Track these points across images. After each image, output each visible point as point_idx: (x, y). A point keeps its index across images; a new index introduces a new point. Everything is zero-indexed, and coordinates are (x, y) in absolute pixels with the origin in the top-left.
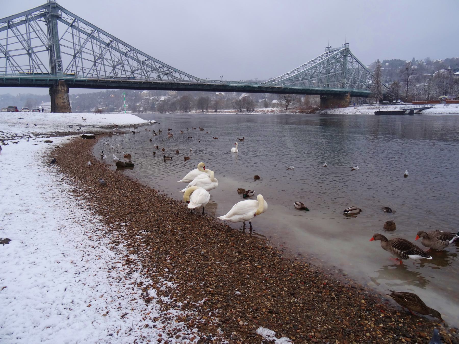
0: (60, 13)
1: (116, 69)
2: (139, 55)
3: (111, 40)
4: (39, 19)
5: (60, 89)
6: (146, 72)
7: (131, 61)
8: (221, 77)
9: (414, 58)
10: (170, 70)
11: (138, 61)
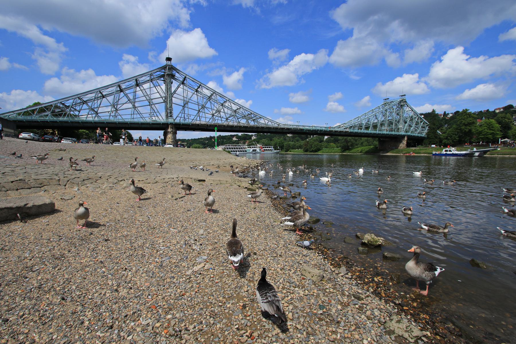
0: (174, 73)
2: (233, 105)
3: (212, 93)
6: (238, 119)
7: (226, 110)
10: (255, 117)
11: (231, 109)
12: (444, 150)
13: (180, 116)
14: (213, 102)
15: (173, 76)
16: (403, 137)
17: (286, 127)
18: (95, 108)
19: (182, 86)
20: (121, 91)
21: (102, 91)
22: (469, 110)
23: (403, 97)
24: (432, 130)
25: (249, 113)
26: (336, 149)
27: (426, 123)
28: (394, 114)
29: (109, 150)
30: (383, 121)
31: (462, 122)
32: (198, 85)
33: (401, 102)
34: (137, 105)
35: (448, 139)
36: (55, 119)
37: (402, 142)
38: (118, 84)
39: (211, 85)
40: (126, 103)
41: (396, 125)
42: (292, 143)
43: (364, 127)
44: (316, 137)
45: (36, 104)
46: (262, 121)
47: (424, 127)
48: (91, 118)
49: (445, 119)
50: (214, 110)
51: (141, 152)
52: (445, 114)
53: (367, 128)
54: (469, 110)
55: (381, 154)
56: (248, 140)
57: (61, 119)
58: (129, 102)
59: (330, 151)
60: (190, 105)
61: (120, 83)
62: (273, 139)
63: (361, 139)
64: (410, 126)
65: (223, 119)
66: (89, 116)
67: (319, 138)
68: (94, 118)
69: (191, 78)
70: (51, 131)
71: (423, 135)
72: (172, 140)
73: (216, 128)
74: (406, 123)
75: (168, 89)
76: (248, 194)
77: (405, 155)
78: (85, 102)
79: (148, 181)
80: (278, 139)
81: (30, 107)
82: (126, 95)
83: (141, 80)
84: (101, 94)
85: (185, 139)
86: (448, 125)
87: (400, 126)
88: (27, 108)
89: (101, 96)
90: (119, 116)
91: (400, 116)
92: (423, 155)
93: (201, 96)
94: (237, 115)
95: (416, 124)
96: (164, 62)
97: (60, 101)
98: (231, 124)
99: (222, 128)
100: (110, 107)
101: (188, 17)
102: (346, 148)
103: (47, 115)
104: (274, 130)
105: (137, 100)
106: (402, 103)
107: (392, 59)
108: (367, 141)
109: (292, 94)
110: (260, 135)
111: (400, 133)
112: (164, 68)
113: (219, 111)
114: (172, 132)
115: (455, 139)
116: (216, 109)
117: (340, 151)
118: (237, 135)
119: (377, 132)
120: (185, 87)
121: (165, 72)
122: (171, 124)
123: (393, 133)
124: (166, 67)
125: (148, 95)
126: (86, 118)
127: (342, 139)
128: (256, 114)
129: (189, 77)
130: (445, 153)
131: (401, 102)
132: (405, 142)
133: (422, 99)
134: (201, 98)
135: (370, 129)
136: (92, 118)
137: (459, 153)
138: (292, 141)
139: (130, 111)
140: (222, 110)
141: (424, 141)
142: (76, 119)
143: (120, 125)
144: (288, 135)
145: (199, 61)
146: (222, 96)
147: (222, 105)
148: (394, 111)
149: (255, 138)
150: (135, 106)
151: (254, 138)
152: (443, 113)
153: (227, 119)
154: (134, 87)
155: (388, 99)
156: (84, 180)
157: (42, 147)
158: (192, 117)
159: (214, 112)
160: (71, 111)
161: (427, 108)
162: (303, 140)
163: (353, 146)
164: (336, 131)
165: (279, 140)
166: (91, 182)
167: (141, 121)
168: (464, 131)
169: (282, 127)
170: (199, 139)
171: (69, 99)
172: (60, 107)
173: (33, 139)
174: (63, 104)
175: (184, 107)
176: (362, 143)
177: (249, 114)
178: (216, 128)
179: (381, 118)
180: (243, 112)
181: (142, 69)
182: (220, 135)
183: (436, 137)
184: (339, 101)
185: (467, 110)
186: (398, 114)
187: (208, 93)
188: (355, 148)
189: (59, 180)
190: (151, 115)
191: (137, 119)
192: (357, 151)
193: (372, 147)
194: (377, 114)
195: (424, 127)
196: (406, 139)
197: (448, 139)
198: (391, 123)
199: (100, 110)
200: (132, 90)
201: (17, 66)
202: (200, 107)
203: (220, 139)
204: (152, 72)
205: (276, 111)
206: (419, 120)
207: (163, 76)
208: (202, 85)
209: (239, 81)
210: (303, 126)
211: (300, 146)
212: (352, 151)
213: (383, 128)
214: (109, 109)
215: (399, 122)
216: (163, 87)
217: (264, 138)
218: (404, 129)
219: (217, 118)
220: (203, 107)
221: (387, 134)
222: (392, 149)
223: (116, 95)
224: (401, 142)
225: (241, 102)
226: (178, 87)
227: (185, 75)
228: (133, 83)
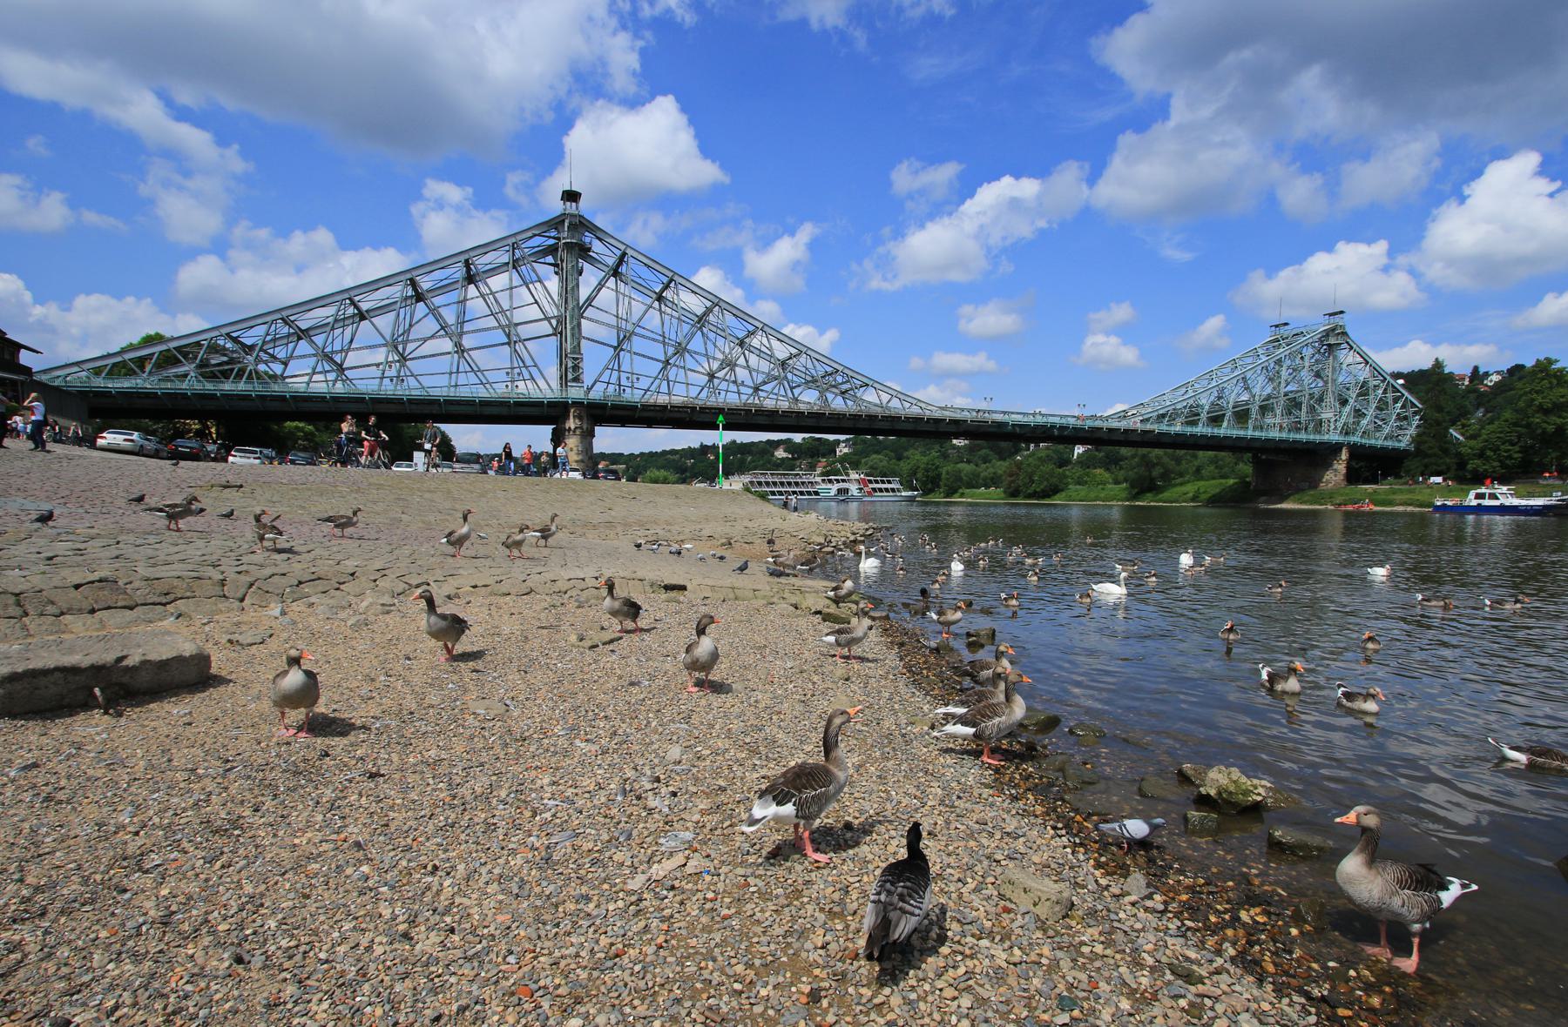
0: (587, 240)
1: (715, 380)
2: (775, 343)
3: (709, 304)
4: (542, 260)
5: (573, 427)
7: (753, 360)
8: (988, 399)
9: (1437, 359)
10: (849, 383)
11: (771, 357)
12: (1472, 494)
13: (605, 378)
14: (711, 335)
15: (583, 251)
16: (1335, 449)
17: (948, 415)
18: (337, 352)
19: (611, 282)
20: (419, 297)
21: (357, 299)
22: (1557, 361)
23: (1338, 320)
24: (1433, 429)
25: (829, 370)
26: (1111, 490)
27: (1413, 405)
28: (1307, 376)
29: (379, 487)
30: (1269, 397)
31: (1533, 400)
32: (665, 280)
33: (1327, 335)
34: (467, 342)
35: (1487, 459)
36: (209, 386)
37: (1331, 465)
38: (409, 276)
39: (707, 278)
40: (433, 337)
41: (1312, 409)
42: (966, 468)
43: (1204, 416)
44: (1047, 448)
45: (150, 340)
46: (870, 396)
47: (1406, 418)
48: (324, 386)
49: (1476, 391)
50: (714, 358)
51: (482, 495)
52: (1477, 376)
53: (1216, 420)
54: (1557, 361)
55: (1263, 506)
56: (824, 456)
57: (228, 386)
58: (442, 332)
59: (1092, 495)
60: (637, 344)
61: (415, 273)
62: (905, 454)
63: (1195, 457)
64: (1359, 414)
65: (743, 389)
66: (316, 378)
67: (1054, 451)
68: (331, 384)
69: (640, 257)
70: (195, 425)
71: (1402, 445)
72: (580, 457)
73: (721, 418)
74: (1344, 402)
75: (569, 291)
76: (826, 631)
77: (1343, 508)
78: (303, 334)
79: (504, 588)
80: (923, 454)
81: (131, 348)
82: (434, 312)
83: (482, 262)
84: (356, 307)
85: (621, 455)
86: (1487, 412)
87: (1327, 414)
88: (123, 351)
89: (354, 315)
90: (411, 379)
91: (1326, 382)
92: (1401, 509)
93: (674, 313)
94: (789, 376)
95: (1378, 408)
96: (557, 207)
97: (224, 331)
98: (769, 404)
99: (740, 419)
100: (384, 350)
101: (633, 61)
102: (1144, 486)
103: (186, 376)
104: (910, 427)
105: (467, 327)
106: (1333, 340)
107: (1299, 193)
108: (1214, 461)
109: (967, 309)
110: (864, 442)
111: (1326, 438)
112: (556, 223)
113: (730, 364)
114: (578, 432)
115: (1510, 457)
116: (721, 356)
117: (1124, 495)
118: (789, 441)
119: (1250, 433)
120: (622, 286)
121: (559, 239)
122: (577, 404)
123: (1302, 436)
124: (564, 221)
125: (503, 311)
126: (308, 384)
127: (1133, 456)
128: (850, 373)
129: (635, 254)
130: (1474, 503)
131: (1327, 334)
132: (1340, 466)
133: (1398, 324)
134: (675, 321)
135: (1225, 424)
136: (324, 385)
137: (1524, 502)
138: (969, 462)
139: (445, 363)
140: (741, 361)
141: (1407, 463)
142: (276, 388)
143: (413, 407)
144: (955, 441)
145: (666, 201)
146: (739, 315)
147: (741, 343)
148: (1307, 364)
149: (846, 450)
150: (461, 345)
151: (843, 450)
152: (1468, 372)
153: (757, 389)
154: (459, 285)
155: (1286, 324)
156: (300, 583)
157: (168, 476)
158: (644, 383)
159: (715, 365)
160: (258, 360)
161: (1415, 356)
162: (1002, 458)
163: (1168, 478)
164: (1111, 430)
165: (925, 459)
166: (321, 589)
167: (482, 393)
168: (1539, 431)
169: (938, 414)
170: (664, 453)
171: (252, 324)
172: (224, 348)
173: (139, 452)
174: (235, 340)
175: (618, 348)
176: (1198, 470)
177: (827, 374)
178: (721, 418)
179: (1261, 388)
180: (809, 365)
181: (486, 228)
182: (734, 442)
183: (1446, 451)
184: (1124, 332)
185: (1549, 361)
186: (1318, 375)
187: (696, 305)
188: (1175, 485)
189: (223, 583)
190: (512, 376)
191: (472, 387)
192: (1181, 496)
193: (1231, 481)
194: (1248, 375)
195: (1406, 418)
196: (1344, 455)
197: (1487, 459)
198: (1294, 404)
199: (352, 359)
200: (454, 296)
201: (91, 217)
202: (671, 350)
203: (734, 455)
204: (519, 237)
205: (916, 362)
206: (1390, 395)
207: (552, 250)
208: (676, 278)
209: (795, 265)
210: (1005, 413)
211: (992, 479)
212: (1166, 495)
213: (1269, 420)
214: (380, 355)
215: (1321, 400)
216: (553, 284)
217: (877, 452)
218: (1340, 425)
219: (724, 385)
220: (681, 350)
221: (1281, 441)
222: (1299, 490)
223: (402, 310)
224: (1327, 465)
225: (801, 333)
226: (600, 286)
227: (623, 247)
228: (458, 272)
